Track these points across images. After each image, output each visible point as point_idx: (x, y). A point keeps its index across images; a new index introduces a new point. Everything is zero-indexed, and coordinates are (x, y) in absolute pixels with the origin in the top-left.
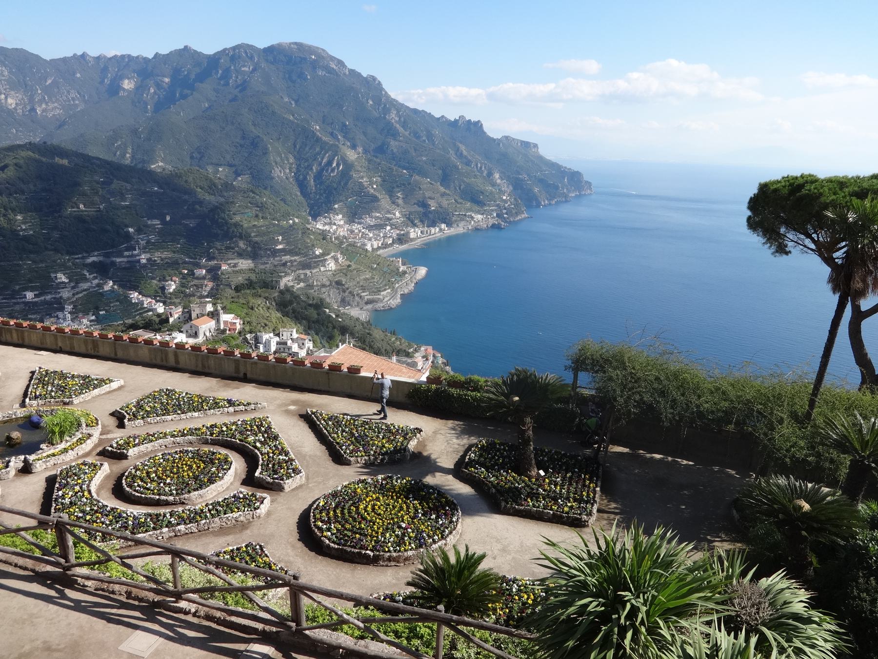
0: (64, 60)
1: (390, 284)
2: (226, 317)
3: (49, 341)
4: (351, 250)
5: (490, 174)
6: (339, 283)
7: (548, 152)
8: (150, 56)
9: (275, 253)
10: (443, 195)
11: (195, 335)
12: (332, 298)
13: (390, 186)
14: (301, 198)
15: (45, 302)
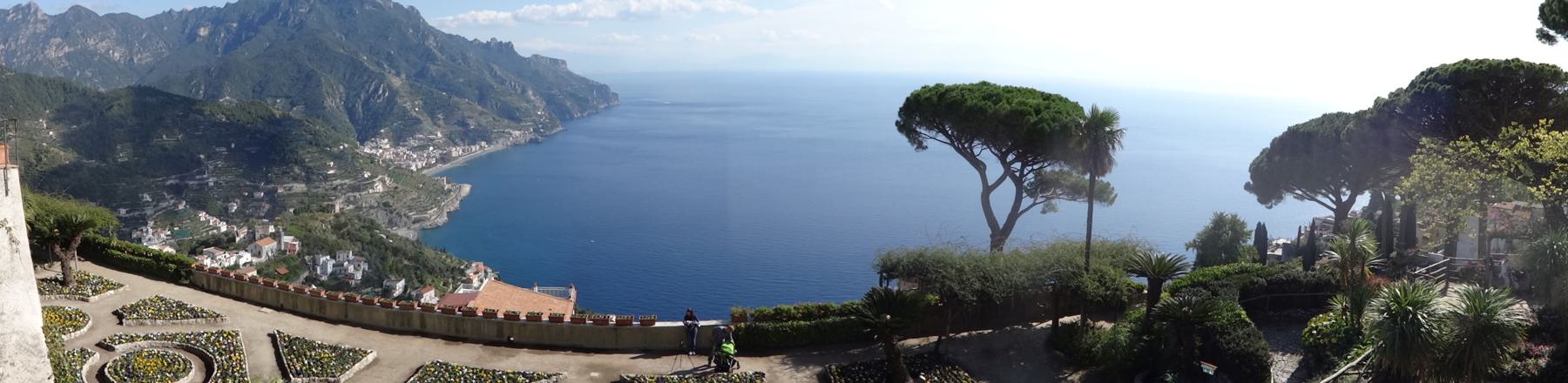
0: (156, 17)
1: (437, 203)
2: (287, 239)
3: (270, 298)
4: (398, 172)
5: (524, 91)
6: (386, 205)
7: (576, 68)
8: (222, 6)
9: (326, 178)
10: (481, 114)
11: (259, 255)
12: (381, 218)
13: (431, 109)
14: (350, 125)
15: (133, 218)
